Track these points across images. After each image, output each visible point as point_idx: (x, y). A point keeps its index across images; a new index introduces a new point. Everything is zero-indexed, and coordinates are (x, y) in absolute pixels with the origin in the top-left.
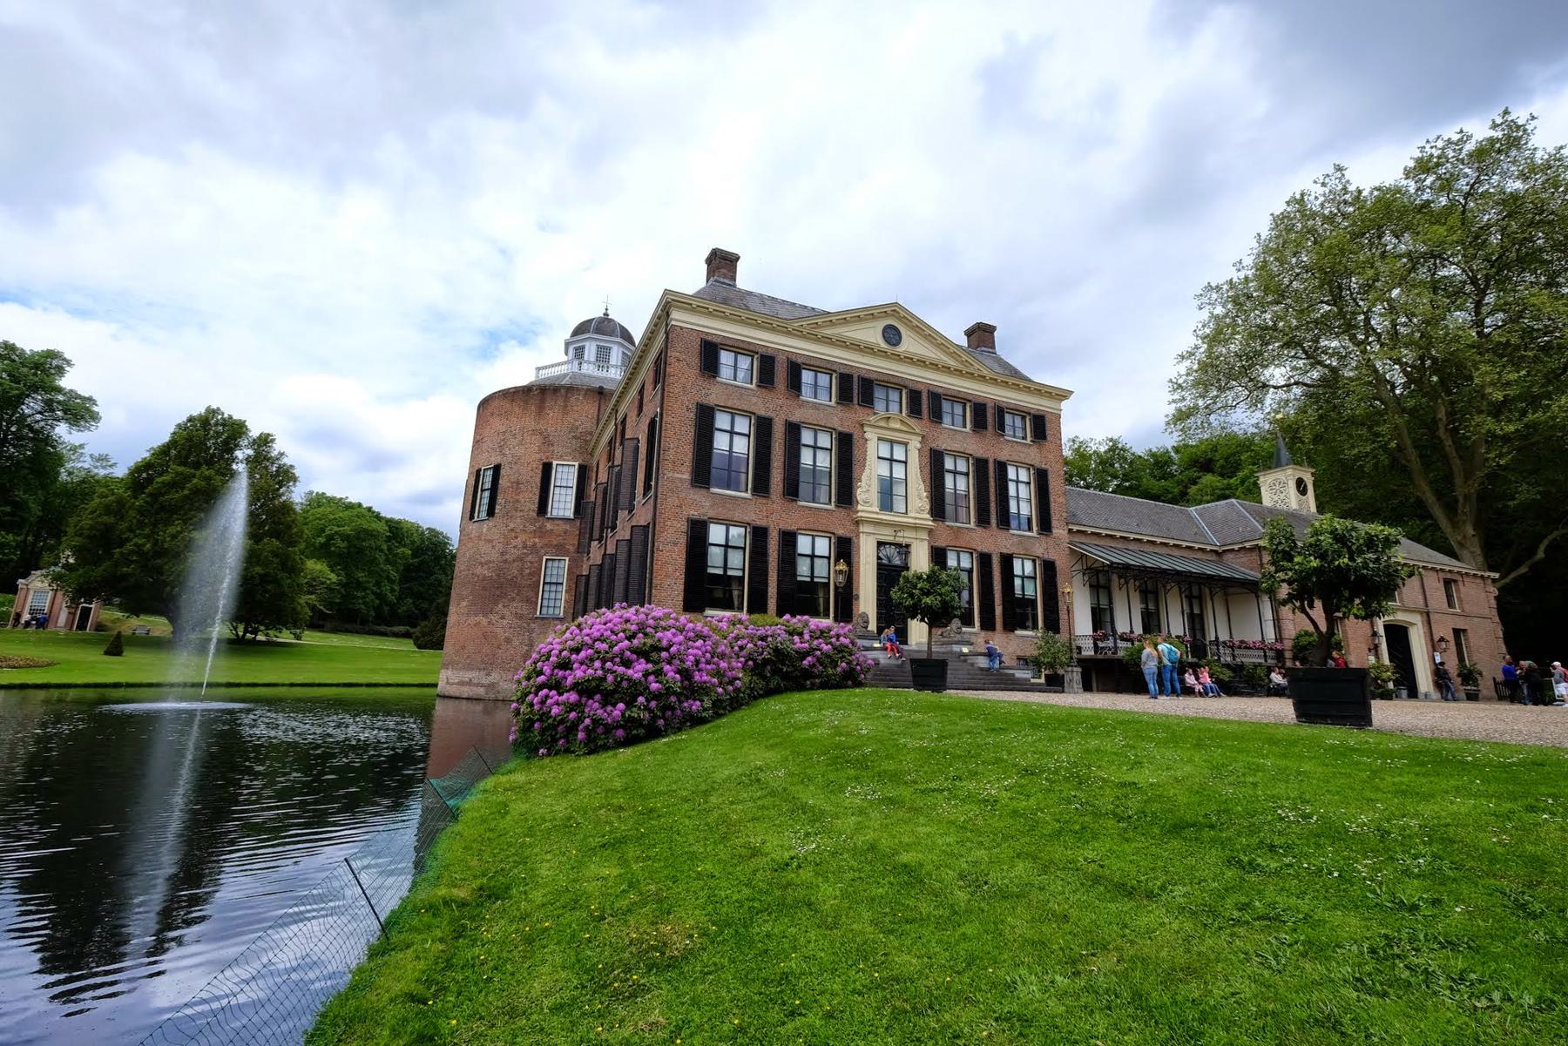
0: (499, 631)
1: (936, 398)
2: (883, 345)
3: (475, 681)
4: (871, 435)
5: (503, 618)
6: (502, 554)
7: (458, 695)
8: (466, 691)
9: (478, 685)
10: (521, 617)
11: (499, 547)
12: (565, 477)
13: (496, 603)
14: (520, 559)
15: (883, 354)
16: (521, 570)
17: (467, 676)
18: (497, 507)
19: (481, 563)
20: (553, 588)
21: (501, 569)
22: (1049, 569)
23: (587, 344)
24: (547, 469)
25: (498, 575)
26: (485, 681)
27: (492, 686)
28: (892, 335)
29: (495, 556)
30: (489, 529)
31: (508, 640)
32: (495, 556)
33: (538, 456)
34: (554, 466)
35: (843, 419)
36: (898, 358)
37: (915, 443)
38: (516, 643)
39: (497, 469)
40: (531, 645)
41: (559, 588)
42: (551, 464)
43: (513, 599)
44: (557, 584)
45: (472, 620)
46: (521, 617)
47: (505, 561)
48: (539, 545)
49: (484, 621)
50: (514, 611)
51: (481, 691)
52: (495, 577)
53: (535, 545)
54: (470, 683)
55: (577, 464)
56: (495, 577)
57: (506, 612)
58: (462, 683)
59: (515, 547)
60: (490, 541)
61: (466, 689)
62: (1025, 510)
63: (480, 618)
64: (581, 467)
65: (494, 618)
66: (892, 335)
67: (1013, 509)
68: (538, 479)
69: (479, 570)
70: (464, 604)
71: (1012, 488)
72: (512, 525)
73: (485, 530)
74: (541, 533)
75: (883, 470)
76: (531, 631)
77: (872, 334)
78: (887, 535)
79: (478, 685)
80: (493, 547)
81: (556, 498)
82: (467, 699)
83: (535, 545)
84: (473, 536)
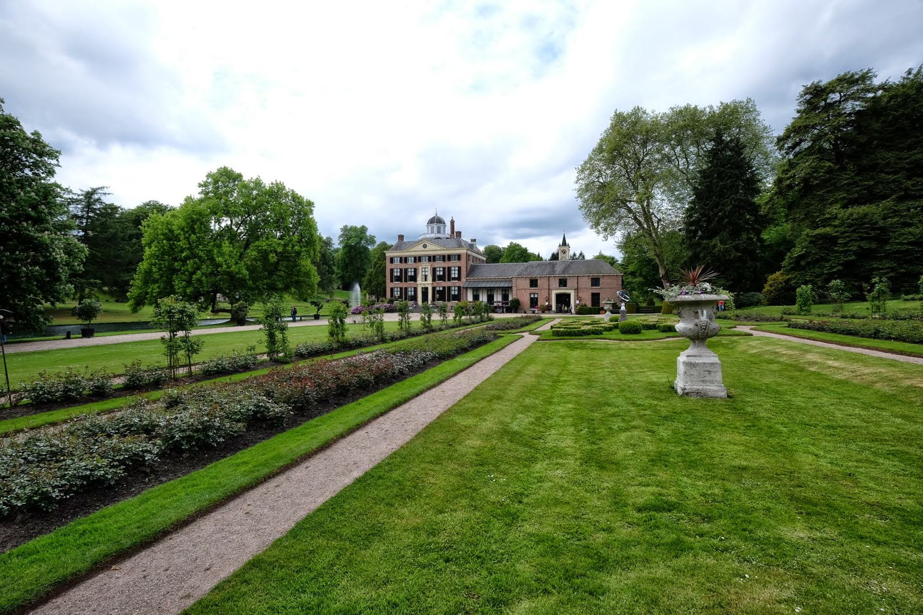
1: (434, 257)
2: (423, 249)
4: (420, 268)
15: (424, 251)
22: (459, 288)
28: (425, 246)
35: (415, 265)
36: (427, 251)
37: (429, 267)
62: (456, 276)
66: (425, 246)
67: (453, 276)
71: (453, 272)
75: (424, 274)
77: (420, 247)
78: (423, 286)
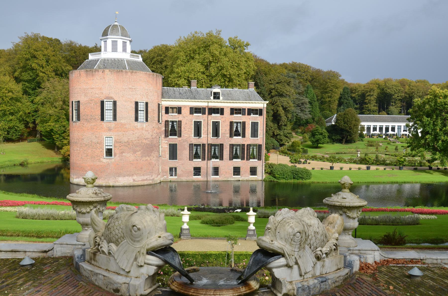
0: (153, 161)
3: (148, 179)
5: (154, 157)
6: (152, 136)
7: (143, 184)
8: (146, 183)
9: (149, 180)
11: (151, 133)
13: (152, 152)
14: (156, 137)
17: (145, 177)
18: (149, 118)
19: (144, 139)
21: (152, 141)
25: (151, 143)
26: (151, 178)
27: (153, 179)
29: (149, 136)
30: (146, 126)
32: (149, 136)
39: (147, 104)
45: (144, 159)
47: (153, 138)
49: (149, 159)
51: (151, 182)
54: (147, 180)
60: (148, 131)
61: (146, 182)
63: (147, 158)
65: (152, 158)
69: (144, 141)
70: (139, 153)
72: (153, 126)
73: (145, 126)
74: (159, 128)
79: (149, 180)
80: (149, 133)
84: (139, 127)
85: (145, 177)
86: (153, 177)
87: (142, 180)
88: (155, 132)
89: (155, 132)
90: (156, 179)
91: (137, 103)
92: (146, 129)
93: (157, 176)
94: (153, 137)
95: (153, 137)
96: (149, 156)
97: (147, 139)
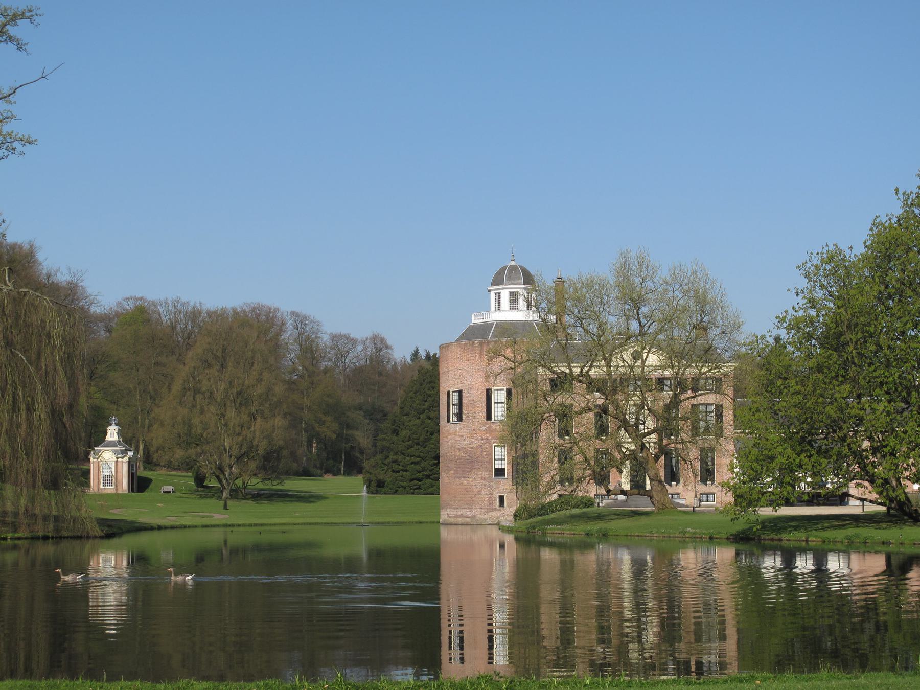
5: (475, 479)
8: (460, 520)
9: (466, 517)
10: (485, 479)
12: (499, 397)
14: (480, 446)
16: (482, 453)
17: (459, 512)
20: (500, 462)
23: (502, 291)
24: (489, 393)
25: (469, 456)
26: (469, 514)
27: (474, 517)
30: (460, 429)
31: (479, 493)
33: (483, 385)
34: (493, 390)
38: (483, 492)
39: (460, 392)
40: (492, 494)
41: (503, 461)
42: (491, 389)
43: (479, 470)
44: (501, 459)
46: (485, 479)
47: (472, 448)
48: (490, 438)
50: (480, 476)
51: (468, 520)
52: (468, 457)
53: (487, 438)
54: (461, 516)
55: (505, 388)
56: (468, 457)
57: (475, 476)
58: (457, 516)
59: (476, 439)
60: (462, 436)
64: (507, 389)
68: (484, 399)
69: (458, 453)
74: (489, 430)
76: (490, 486)
81: (496, 410)
82: (461, 524)
83: (487, 438)
85: (459, 512)
86: (474, 512)
87: (455, 517)
88: (478, 436)
89: (478, 436)
90: (480, 516)
91: (449, 392)
92: (460, 434)
93: (486, 513)
94: (473, 445)
95: (473, 445)
96: (465, 478)
97: (462, 449)
